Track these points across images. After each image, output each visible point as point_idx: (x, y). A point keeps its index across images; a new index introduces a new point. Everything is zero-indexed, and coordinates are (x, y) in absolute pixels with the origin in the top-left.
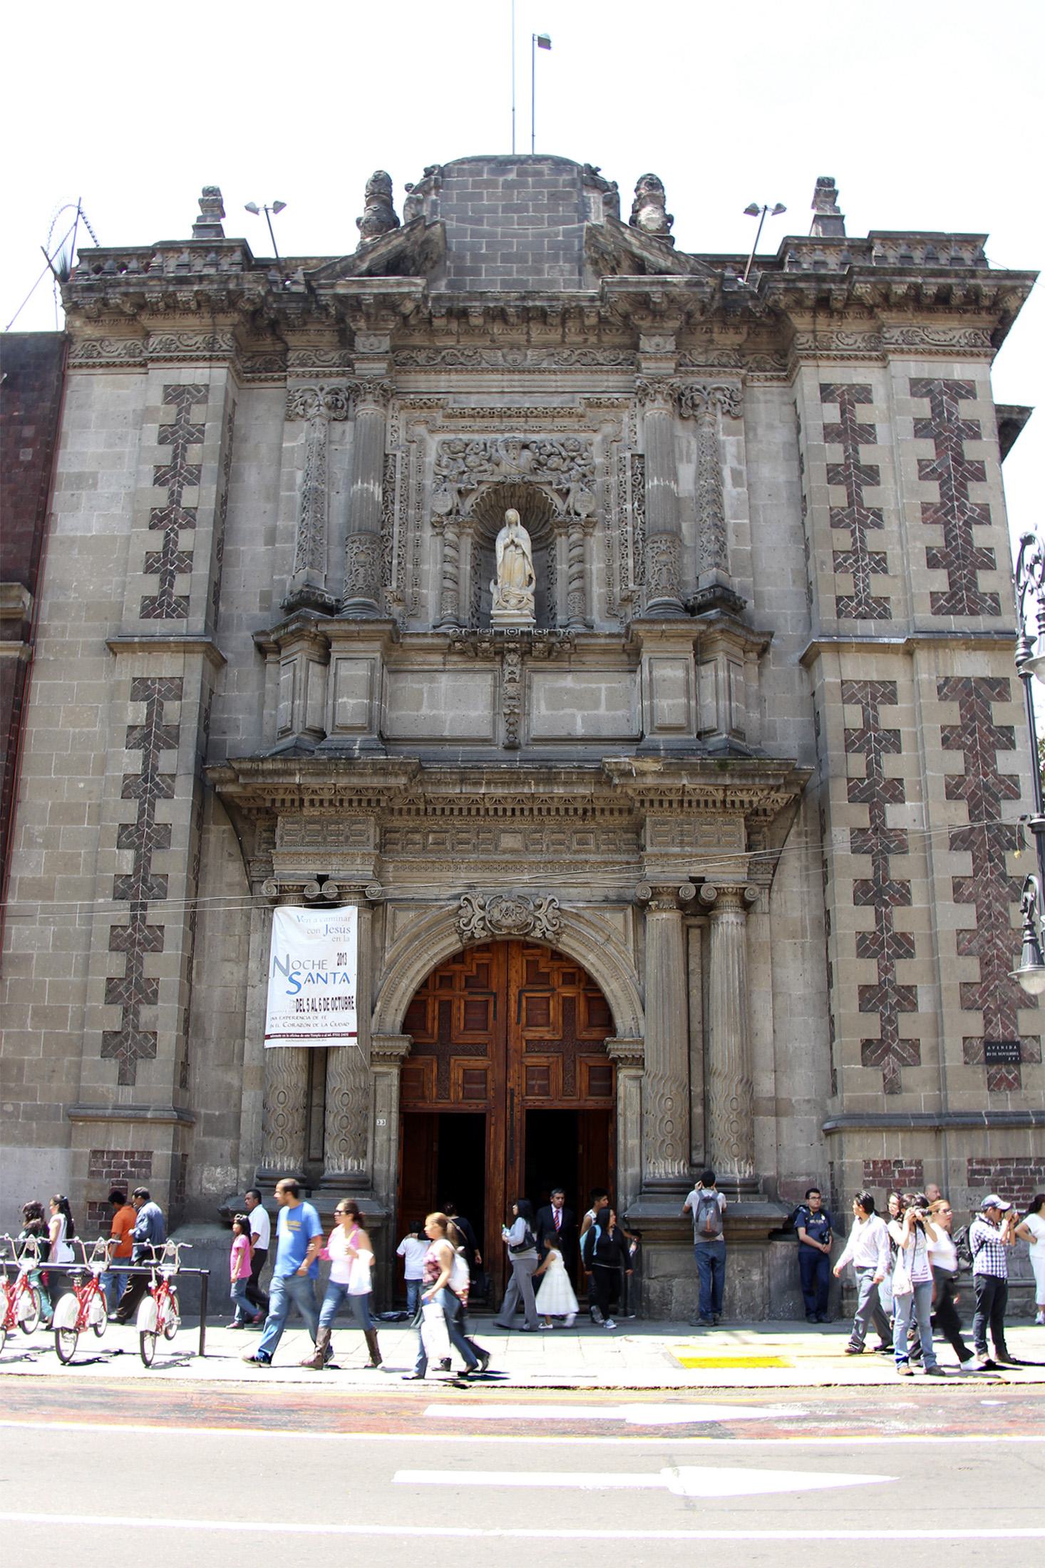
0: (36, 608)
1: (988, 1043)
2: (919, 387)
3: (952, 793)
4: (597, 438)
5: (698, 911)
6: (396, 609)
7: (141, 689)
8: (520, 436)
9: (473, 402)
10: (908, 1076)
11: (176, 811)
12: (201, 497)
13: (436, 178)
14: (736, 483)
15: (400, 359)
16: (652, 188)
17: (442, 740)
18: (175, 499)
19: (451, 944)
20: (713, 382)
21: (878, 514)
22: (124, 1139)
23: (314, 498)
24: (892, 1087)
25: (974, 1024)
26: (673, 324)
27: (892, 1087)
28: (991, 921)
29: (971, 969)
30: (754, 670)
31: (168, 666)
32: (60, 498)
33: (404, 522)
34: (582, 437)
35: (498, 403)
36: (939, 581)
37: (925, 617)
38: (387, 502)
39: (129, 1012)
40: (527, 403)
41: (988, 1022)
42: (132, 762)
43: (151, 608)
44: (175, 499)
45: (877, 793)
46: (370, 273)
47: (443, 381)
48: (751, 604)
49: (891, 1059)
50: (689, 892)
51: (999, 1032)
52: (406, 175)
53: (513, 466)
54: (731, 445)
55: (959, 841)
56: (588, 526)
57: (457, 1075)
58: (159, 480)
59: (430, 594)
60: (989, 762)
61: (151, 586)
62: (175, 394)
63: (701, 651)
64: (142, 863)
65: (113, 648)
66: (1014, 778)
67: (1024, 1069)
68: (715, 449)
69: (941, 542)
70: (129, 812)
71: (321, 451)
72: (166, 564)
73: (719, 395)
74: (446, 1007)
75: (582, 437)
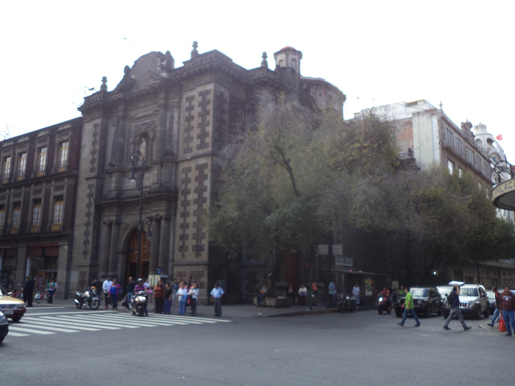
1: (197, 246)
2: (201, 94)
3: (196, 192)
4: (156, 119)
5: (159, 221)
7: (90, 187)
8: (145, 122)
10: (186, 254)
11: (92, 210)
12: (97, 147)
13: (136, 62)
14: (176, 124)
16: (168, 53)
19: (129, 231)
20: (174, 101)
21: (193, 127)
22: (84, 270)
23: (114, 143)
24: (183, 256)
25: (194, 242)
27: (183, 256)
29: (195, 230)
30: (174, 168)
32: (82, 149)
34: (154, 119)
37: (195, 152)
39: (86, 247)
41: (197, 242)
42: (87, 200)
43: (92, 170)
45: (187, 192)
46: (117, 94)
47: (134, 112)
48: (175, 152)
50: (155, 217)
51: (199, 244)
53: (143, 129)
54: (176, 115)
55: (196, 202)
56: (154, 138)
58: (93, 144)
60: (203, 183)
61: (91, 166)
62: (95, 126)
63: (162, 167)
64: (88, 219)
65: (87, 179)
68: (172, 117)
70: (87, 210)
72: (93, 162)
73: (175, 104)
75: (154, 119)
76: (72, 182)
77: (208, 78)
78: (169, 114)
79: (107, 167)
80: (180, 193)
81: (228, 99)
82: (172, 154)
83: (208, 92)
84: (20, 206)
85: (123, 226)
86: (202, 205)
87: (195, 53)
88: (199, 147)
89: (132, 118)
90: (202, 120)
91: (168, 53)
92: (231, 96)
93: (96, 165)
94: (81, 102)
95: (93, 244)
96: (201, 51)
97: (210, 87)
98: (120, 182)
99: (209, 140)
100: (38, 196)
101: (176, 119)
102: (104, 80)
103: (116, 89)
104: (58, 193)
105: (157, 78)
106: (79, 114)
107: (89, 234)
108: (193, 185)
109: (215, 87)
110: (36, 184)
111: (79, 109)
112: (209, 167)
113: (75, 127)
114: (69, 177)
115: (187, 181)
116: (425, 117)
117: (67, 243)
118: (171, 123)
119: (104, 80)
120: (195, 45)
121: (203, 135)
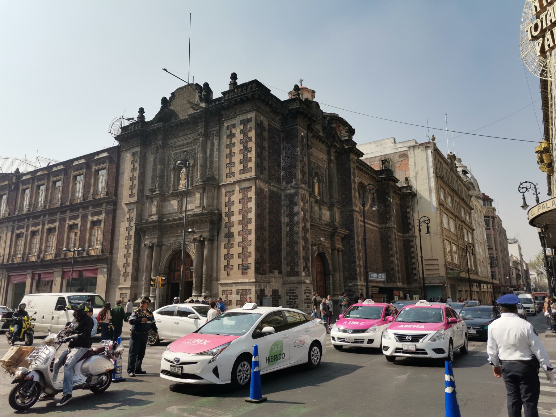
0: (117, 199)
4: (196, 147)
5: (202, 242)
6: (167, 189)
8: (185, 149)
9: (177, 144)
10: (231, 272)
11: (132, 233)
15: (165, 139)
16: (206, 85)
17: (171, 214)
18: (133, 175)
19: (170, 252)
20: (213, 129)
21: (234, 153)
24: (228, 275)
25: (240, 261)
26: (203, 120)
28: (244, 239)
30: (216, 191)
31: (132, 207)
33: (168, 171)
34: (194, 147)
35: (180, 143)
36: (241, 167)
37: (238, 176)
38: (165, 168)
40: (185, 142)
44: (133, 175)
45: (230, 214)
47: (173, 141)
48: (217, 177)
49: (229, 269)
52: (168, 97)
54: (216, 142)
55: (240, 223)
56: (195, 165)
57: (176, 276)
59: (172, 185)
63: (204, 191)
66: (251, 208)
67: (248, 270)
68: (213, 145)
69: (242, 158)
71: (155, 160)
74: (175, 263)
75: (194, 147)
76: (111, 207)
77: (248, 106)
78: (209, 142)
79: (147, 193)
80: (223, 215)
81: (267, 128)
82: (214, 179)
83: (249, 120)
84: (55, 232)
85: (164, 247)
86: (247, 226)
87: (233, 84)
88: (242, 172)
89: (172, 146)
90: (244, 147)
91: (206, 85)
92: (269, 125)
93: (135, 191)
94: (117, 131)
95: (133, 266)
96: (239, 82)
97: (252, 115)
98: (160, 207)
99: (252, 165)
100: (75, 222)
101: (216, 146)
102: (142, 111)
103: (154, 119)
104: (96, 218)
105: (197, 108)
106: (116, 143)
107: (129, 257)
108: (237, 207)
109: (256, 115)
110: (71, 211)
111: (116, 138)
112: (253, 189)
113: (113, 156)
114: (108, 203)
115: (230, 203)
116: (420, 149)
117: (106, 266)
118: (212, 150)
119: (142, 111)
120: (234, 76)
121: (245, 161)
